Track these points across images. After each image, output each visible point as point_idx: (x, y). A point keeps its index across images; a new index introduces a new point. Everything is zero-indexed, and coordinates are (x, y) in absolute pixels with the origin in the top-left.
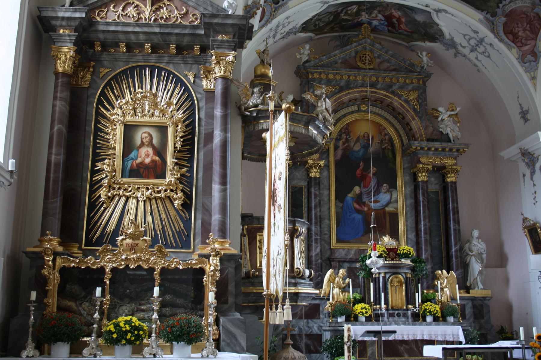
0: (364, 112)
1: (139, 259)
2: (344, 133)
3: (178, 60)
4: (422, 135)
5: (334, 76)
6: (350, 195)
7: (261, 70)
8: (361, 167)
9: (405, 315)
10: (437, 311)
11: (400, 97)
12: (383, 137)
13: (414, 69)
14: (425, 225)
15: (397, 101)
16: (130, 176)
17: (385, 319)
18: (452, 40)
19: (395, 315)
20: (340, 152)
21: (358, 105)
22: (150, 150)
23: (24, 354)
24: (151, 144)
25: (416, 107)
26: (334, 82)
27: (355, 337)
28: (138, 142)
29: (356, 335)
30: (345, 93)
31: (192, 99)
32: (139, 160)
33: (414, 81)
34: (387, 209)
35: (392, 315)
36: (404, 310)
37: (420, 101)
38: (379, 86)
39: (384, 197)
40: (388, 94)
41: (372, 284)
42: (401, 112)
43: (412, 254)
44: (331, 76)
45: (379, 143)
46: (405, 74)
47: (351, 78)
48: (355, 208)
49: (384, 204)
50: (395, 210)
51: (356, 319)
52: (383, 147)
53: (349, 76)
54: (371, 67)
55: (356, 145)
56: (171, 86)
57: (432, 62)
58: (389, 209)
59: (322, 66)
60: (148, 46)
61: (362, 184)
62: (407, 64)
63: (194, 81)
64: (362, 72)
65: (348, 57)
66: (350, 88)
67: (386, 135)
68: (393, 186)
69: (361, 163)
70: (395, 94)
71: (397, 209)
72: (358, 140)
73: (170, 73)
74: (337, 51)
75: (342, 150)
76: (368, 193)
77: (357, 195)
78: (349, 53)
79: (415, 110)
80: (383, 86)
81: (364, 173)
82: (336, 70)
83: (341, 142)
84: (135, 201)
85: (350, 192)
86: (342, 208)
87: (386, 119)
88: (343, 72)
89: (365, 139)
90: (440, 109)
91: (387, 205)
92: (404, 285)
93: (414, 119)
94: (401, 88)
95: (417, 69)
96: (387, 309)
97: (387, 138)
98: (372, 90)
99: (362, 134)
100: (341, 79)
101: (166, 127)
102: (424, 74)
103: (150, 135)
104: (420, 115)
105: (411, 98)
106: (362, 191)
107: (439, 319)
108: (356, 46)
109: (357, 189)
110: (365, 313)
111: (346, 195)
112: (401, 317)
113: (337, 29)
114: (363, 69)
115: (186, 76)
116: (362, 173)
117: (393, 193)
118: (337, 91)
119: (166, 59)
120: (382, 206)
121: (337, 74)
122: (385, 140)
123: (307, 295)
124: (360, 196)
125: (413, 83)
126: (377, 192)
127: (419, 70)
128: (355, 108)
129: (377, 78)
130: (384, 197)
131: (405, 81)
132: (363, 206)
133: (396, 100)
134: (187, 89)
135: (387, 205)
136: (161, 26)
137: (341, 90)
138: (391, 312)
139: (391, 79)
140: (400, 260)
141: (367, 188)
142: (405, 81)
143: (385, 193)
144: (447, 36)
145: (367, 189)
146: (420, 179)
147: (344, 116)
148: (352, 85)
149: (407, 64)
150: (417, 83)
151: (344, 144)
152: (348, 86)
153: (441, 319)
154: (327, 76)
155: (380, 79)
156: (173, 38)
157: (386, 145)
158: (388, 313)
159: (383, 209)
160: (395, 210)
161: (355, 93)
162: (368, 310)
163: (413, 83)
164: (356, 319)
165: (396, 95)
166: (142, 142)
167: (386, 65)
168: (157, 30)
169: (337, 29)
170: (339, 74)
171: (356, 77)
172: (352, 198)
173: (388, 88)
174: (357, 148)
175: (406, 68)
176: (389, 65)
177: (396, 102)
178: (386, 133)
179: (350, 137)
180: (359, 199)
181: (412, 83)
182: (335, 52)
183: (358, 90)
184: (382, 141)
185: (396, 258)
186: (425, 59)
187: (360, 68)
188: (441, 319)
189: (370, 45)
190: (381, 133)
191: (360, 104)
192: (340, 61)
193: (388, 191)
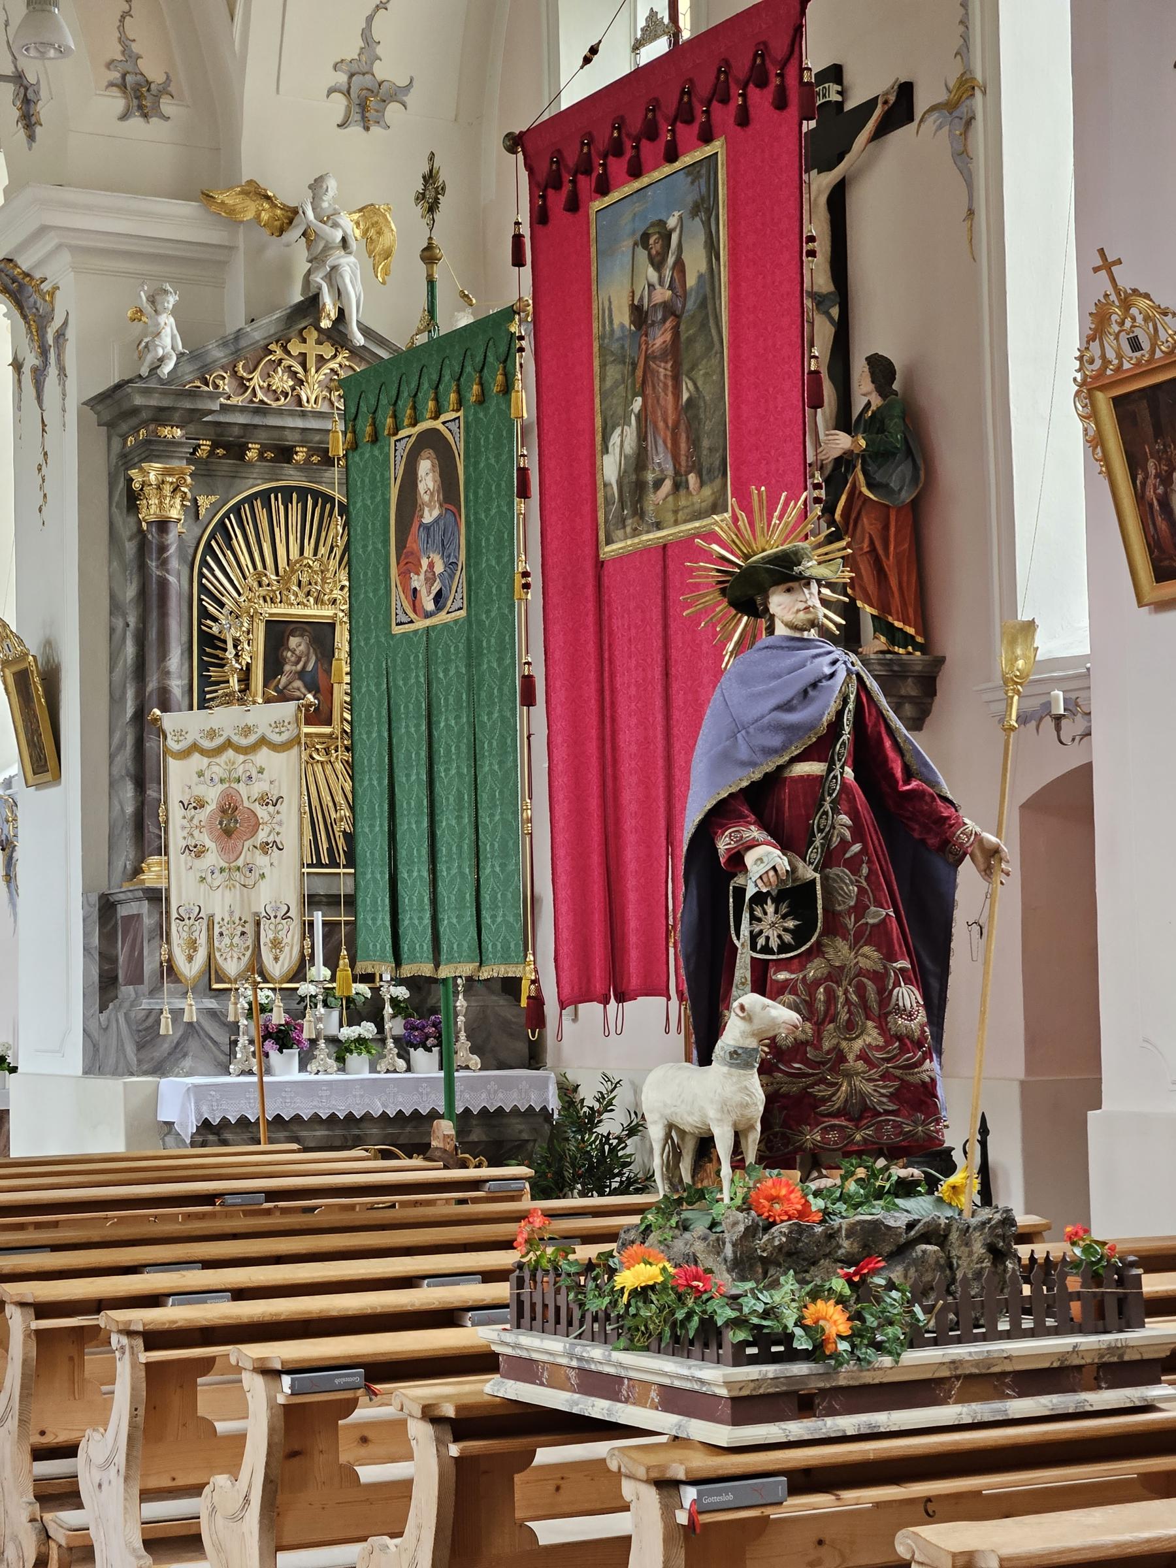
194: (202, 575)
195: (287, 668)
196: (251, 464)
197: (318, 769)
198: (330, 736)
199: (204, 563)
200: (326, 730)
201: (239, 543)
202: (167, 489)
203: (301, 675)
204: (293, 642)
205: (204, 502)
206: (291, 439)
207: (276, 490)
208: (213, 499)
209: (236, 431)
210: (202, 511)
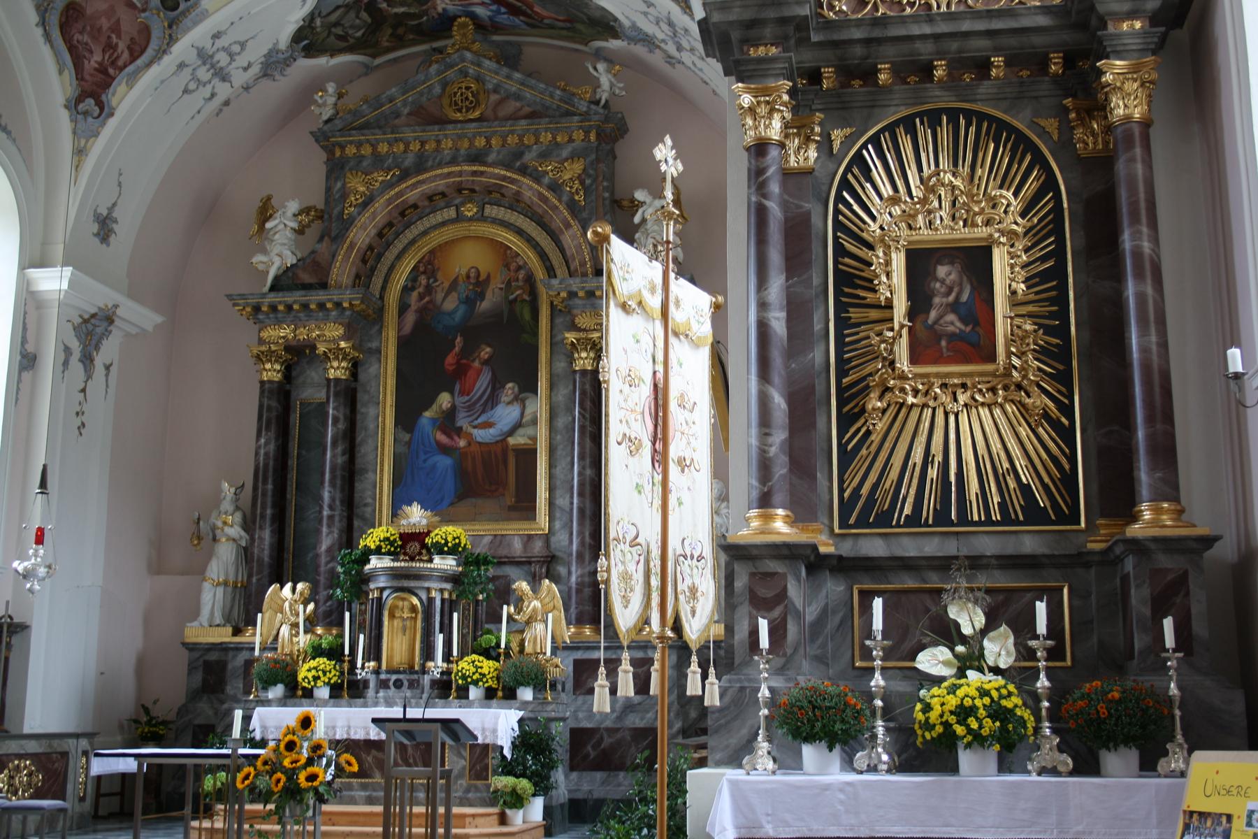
0: (471, 219)
2: (424, 273)
4: (585, 263)
5: (390, 144)
6: (427, 414)
8: (457, 349)
9: (413, 685)
10: (484, 675)
11: (537, 178)
12: (512, 274)
13: (574, 106)
14: (580, 474)
15: (531, 188)
17: (371, 692)
18: (634, 26)
19: (391, 683)
20: (411, 318)
21: (457, 206)
25: (577, 198)
26: (390, 160)
27: (262, 732)
29: (264, 728)
30: (410, 182)
33: (575, 136)
34: (512, 441)
35: (384, 685)
36: (416, 672)
37: (588, 182)
38: (491, 158)
39: (505, 414)
40: (509, 174)
41: (347, 615)
42: (540, 211)
43: (450, 545)
44: (383, 148)
45: (501, 289)
46: (550, 123)
47: (427, 147)
48: (438, 443)
49: (506, 429)
50: (530, 442)
51: (309, 694)
52: (511, 297)
53: (423, 143)
54: (477, 114)
55: (449, 298)
57: (621, 85)
58: (517, 440)
59: (361, 128)
61: (457, 387)
62: (557, 97)
64: (450, 130)
65: (424, 99)
66: (426, 170)
67: (519, 268)
68: (529, 386)
69: (458, 339)
70: (529, 171)
71: (534, 439)
72: (454, 285)
74: (394, 90)
75: (416, 311)
76: (469, 406)
77: (444, 412)
78: (425, 91)
79: (572, 206)
80: (501, 157)
81: (464, 361)
82: (392, 133)
83: (415, 294)
85: (427, 407)
86: (409, 444)
87: (520, 232)
88: (409, 134)
89: (470, 283)
90: (640, 195)
91: (512, 432)
92: (420, 616)
93: (568, 226)
94: (544, 156)
95: (580, 107)
96: (377, 672)
97: (521, 277)
98: (475, 168)
99: (464, 272)
100: (405, 151)
102: (596, 117)
104: (585, 215)
105: (566, 177)
106: (457, 403)
107: (496, 695)
108: (439, 73)
109: (444, 400)
110: (311, 679)
111: (419, 414)
112: (403, 688)
113: (411, 37)
114: (456, 122)
116: (458, 362)
117: (527, 402)
118: (395, 179)
120: (500, 435)
121: (396, 140)
122: (517, 280)
124: (451, 414)
125: (573, 141)
126: (492, 401)
127: (585, 109)
128: (452, 213)
129: (488, 140)
130: (507, 412)
131: (554, 138)
132: (456, 438)
133: (528, 185)
135: (512, 432)
137: (405, 175)
138: (383, 676)
139: (521, 137)
140: (431, 561)
141: (468, 395)
142: (554, 138)
143: (509, 403)
144: (626, 23)
145: (466, 398)
146: (578, 366)
147: (425, 233)
148: (430, 163)
149: (557, 97)
150: (583, 140)
151: (421, 297)
152: (420, 167)
153: (500, 694)
154: (374, 146)
155: (493, 142)
157: (518, 292)
158: (378, 678)
159: (502, 442)
160: (530, 442)
161: (435, 180)
162: (320, 673)
163: (573, 141)
164: (309, 694)
165: (530, 175)
167: (512, 106)
169: (411, 37)
170: (401, 140)
171: (438, 142)
172: (433, 420)
173: (513, 160)
174: (450, 304)
175: (559, 107)
176: (518, 104)
177: (529, 189)
178: (521, 263)
179: (436, 280)
180: (448, 422)
181: (571, 140)
182: (388, 93)
183: (439, 172)
184: (509, 283)
185: (420, 554)
186: (605, 80)
187: (443, 122)
188: (500, 694)
189: (472, 63)
190: (507, 266)
191: (463, 204)
192: (406, 111)
193: (516, 399)
194: (837, 212)
195: (937, 300)
196: (886, 89)
197: (984, 412)
198: (993, 374)
199: (840, 199)
200: (989, 367)
201: (878, 173)
202: (763, 110)
203: (954, 307)
204: (942, 271)
205: (838, 135)
206: (926, 49)
207: (920, 115)
208: (848, 131)
209: (858, 51)
210: (836, 145)
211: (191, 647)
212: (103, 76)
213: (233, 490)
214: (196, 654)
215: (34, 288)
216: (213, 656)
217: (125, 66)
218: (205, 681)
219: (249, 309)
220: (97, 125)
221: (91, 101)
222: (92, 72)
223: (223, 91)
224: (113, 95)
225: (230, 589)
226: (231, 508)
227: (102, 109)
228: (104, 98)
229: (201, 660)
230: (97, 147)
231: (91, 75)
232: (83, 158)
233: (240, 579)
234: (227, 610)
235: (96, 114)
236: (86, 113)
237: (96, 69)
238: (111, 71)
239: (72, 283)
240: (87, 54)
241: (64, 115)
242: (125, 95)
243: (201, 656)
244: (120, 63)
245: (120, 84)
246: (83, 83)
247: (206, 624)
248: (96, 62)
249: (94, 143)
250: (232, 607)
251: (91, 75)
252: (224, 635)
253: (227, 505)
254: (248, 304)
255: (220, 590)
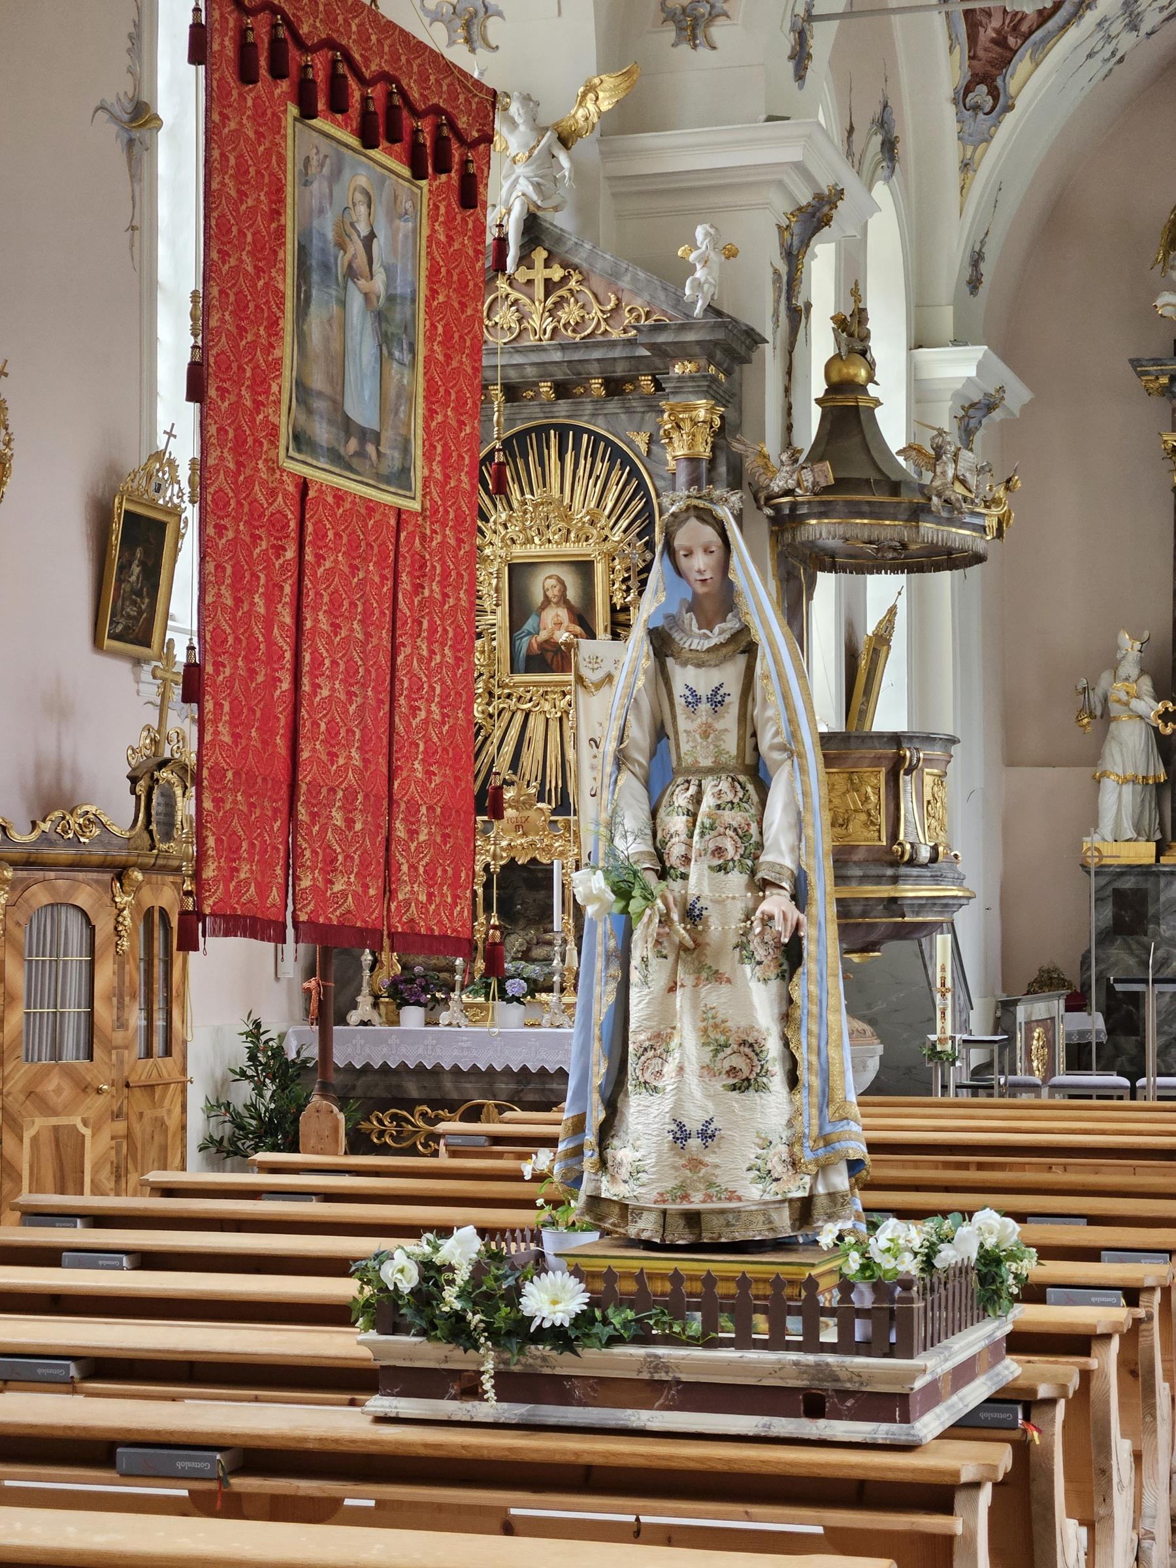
1: (532, 844)
3: (613, 406)
7: (840, 370)
16: (527, 671)
22: (563, 614)
23: (354, 1017)
24: (564, 601)
28: (539, 598)
31: (647, 494)
32: (543, 636)
56: (601, 468)
60: (545, 388)
63: (649, 452)
73: (598, 438)
84: (541, 719)
101: (590, 564)
103: (561, 582)
115: (630, 443)
119: (589, 408)
123: (923, 902)
134: (635, 473)
136: (563, 347)
156: (595, 368)
166: (546, 596)
168: (557, 356)
211: (1101, 870)
212: (998, 49)
213: (1137, 645)
214: (1103, 881)
215: (925, 375)
216: (1128, 883)
217: (1031, 33)
218: (1117, 918)
219: (1164, 380)
220: (988, 124)
221: (983, 88)
222: (988, 44)
223: (1126, 41)
224: (1012, 76)
225: (1139, 788)
226: (1134, 672)
227: (996, 99)
228: (999, 82)
229: (1109, 891)
230: (991, 157)
231: (985, 50)
232: (970, 174)
233: (1152, 774)
234: (1136, 817)
235: (987, 109)
236: (976, 108)
237: (993, 41)
238: (1011, 41)
239: (981, 367)
240: (984, 20)
241: (950, 111)
242: (1032, 73)
243: (1109, 883)
244: (1024, 28)
245: (1021, 61)
246: (975, 62)
247: (1109, 838)
248: (994, 29)
249: (985, 150)
250: (1142, 812)
251: (985, 50)
252: (1144, 852)
253: (1129, 668)
254: (1163, 373)
255: (1128, 790)
